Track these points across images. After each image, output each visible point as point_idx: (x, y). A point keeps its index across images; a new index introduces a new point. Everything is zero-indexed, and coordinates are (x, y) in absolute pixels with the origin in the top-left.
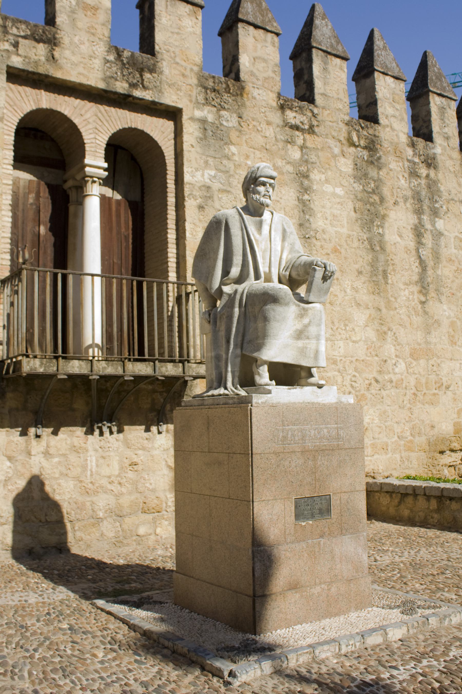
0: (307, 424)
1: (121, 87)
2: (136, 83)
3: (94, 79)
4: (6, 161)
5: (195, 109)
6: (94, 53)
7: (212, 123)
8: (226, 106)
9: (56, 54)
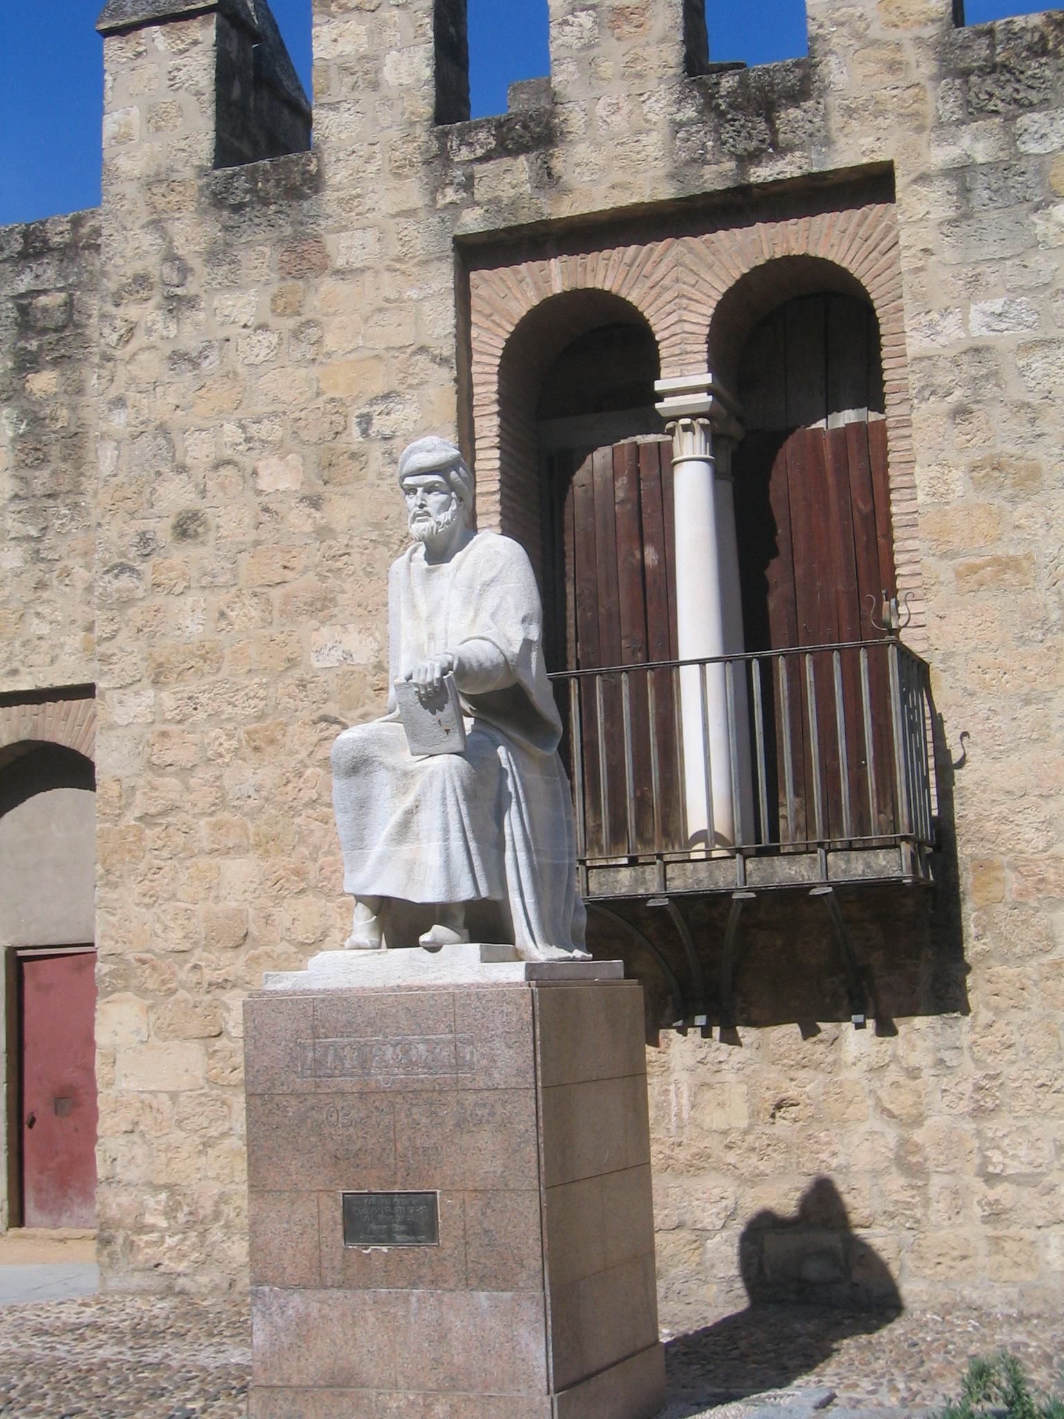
0: (375, 1033)
1: (715, 176)
2: (757, 149)
3: (651, 185)
6: (647, 121)
8: (1034, 96)
9: (557, 165)
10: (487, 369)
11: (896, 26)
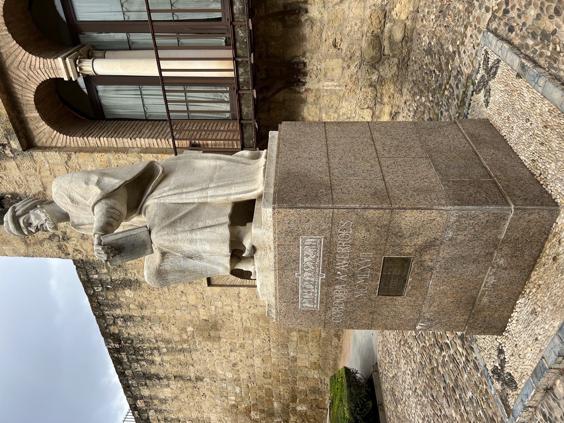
0: (298, 279)
4: (99, 142)
10: (72, 140)
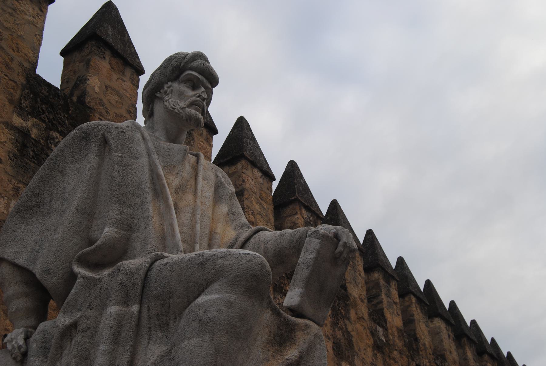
5: (15, 115)
7: (35, 140)
11: (13, 50)
